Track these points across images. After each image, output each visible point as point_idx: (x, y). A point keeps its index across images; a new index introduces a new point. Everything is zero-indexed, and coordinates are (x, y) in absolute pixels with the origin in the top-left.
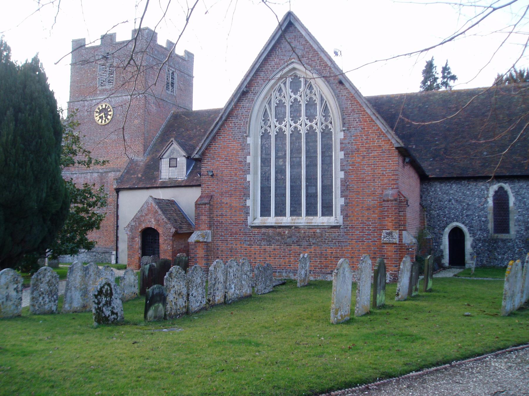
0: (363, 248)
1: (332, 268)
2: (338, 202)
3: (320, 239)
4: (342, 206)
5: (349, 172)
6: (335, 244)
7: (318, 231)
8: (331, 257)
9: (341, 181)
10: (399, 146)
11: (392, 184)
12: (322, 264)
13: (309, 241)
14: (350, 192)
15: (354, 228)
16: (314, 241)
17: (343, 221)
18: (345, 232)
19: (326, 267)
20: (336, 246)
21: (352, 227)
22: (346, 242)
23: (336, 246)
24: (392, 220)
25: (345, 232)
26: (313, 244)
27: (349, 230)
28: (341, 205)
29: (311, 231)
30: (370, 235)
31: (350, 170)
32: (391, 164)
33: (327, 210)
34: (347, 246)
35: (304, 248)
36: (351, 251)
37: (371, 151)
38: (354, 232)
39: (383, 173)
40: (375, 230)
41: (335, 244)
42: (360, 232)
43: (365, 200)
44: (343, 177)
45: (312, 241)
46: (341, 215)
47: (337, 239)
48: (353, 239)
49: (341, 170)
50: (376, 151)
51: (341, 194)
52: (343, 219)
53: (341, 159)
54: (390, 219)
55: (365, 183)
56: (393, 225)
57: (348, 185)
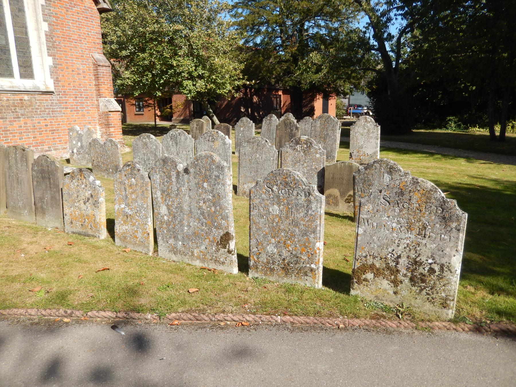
0: (79, 118)
1: (49, 144)
2: (41, 61)
3: (30, 109)
4: (50, 67)
5: (53, 25)
6: (49, 114)
7: (26, 97)
8: (46, 131)
9: (46, 35)
10: (108, 7)
11: (98, 48)
12: (38, 140)
13: (16, 112)
14: (58, 51)
15: (67, 95)
16: (22, 112)
17: (55, 86)
18: (58, 100)
19: (42, 143)
20: (51, 117)
21: (65, 94)
22: (60, 111)
23: (51, 117)
24: (108, 88)
25: (58, 100)
26: (22, 115)
27: (62, 97)
28: (50, 66)
29: (18, 97)
30: (83, 103)
31: (54, 22)
32: (94, 25)
33: (27, 70)
34: (62, 116)
35: (10, 121)
36: (67, 121)
37: (75, 5)
38: (68, 100)
39: (88, 34)
40: (87, 98)
41: (49, 114)
42: (74, 100)
43: (74, 63)
44: (47, 29)
45: (20, 111)
46: (51, 78)
47: (50, 108)
48: (67, 108)
49: (44, 21)
50: (79, 5)
51: (48, 52)
52: (54, 83)
53: (42, 5)
54: (106, 87)
55: (72, 42)
56: (109, 93)
57: (54, 42)
